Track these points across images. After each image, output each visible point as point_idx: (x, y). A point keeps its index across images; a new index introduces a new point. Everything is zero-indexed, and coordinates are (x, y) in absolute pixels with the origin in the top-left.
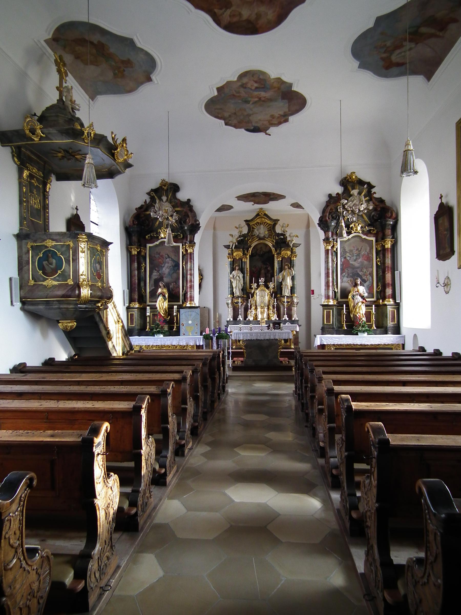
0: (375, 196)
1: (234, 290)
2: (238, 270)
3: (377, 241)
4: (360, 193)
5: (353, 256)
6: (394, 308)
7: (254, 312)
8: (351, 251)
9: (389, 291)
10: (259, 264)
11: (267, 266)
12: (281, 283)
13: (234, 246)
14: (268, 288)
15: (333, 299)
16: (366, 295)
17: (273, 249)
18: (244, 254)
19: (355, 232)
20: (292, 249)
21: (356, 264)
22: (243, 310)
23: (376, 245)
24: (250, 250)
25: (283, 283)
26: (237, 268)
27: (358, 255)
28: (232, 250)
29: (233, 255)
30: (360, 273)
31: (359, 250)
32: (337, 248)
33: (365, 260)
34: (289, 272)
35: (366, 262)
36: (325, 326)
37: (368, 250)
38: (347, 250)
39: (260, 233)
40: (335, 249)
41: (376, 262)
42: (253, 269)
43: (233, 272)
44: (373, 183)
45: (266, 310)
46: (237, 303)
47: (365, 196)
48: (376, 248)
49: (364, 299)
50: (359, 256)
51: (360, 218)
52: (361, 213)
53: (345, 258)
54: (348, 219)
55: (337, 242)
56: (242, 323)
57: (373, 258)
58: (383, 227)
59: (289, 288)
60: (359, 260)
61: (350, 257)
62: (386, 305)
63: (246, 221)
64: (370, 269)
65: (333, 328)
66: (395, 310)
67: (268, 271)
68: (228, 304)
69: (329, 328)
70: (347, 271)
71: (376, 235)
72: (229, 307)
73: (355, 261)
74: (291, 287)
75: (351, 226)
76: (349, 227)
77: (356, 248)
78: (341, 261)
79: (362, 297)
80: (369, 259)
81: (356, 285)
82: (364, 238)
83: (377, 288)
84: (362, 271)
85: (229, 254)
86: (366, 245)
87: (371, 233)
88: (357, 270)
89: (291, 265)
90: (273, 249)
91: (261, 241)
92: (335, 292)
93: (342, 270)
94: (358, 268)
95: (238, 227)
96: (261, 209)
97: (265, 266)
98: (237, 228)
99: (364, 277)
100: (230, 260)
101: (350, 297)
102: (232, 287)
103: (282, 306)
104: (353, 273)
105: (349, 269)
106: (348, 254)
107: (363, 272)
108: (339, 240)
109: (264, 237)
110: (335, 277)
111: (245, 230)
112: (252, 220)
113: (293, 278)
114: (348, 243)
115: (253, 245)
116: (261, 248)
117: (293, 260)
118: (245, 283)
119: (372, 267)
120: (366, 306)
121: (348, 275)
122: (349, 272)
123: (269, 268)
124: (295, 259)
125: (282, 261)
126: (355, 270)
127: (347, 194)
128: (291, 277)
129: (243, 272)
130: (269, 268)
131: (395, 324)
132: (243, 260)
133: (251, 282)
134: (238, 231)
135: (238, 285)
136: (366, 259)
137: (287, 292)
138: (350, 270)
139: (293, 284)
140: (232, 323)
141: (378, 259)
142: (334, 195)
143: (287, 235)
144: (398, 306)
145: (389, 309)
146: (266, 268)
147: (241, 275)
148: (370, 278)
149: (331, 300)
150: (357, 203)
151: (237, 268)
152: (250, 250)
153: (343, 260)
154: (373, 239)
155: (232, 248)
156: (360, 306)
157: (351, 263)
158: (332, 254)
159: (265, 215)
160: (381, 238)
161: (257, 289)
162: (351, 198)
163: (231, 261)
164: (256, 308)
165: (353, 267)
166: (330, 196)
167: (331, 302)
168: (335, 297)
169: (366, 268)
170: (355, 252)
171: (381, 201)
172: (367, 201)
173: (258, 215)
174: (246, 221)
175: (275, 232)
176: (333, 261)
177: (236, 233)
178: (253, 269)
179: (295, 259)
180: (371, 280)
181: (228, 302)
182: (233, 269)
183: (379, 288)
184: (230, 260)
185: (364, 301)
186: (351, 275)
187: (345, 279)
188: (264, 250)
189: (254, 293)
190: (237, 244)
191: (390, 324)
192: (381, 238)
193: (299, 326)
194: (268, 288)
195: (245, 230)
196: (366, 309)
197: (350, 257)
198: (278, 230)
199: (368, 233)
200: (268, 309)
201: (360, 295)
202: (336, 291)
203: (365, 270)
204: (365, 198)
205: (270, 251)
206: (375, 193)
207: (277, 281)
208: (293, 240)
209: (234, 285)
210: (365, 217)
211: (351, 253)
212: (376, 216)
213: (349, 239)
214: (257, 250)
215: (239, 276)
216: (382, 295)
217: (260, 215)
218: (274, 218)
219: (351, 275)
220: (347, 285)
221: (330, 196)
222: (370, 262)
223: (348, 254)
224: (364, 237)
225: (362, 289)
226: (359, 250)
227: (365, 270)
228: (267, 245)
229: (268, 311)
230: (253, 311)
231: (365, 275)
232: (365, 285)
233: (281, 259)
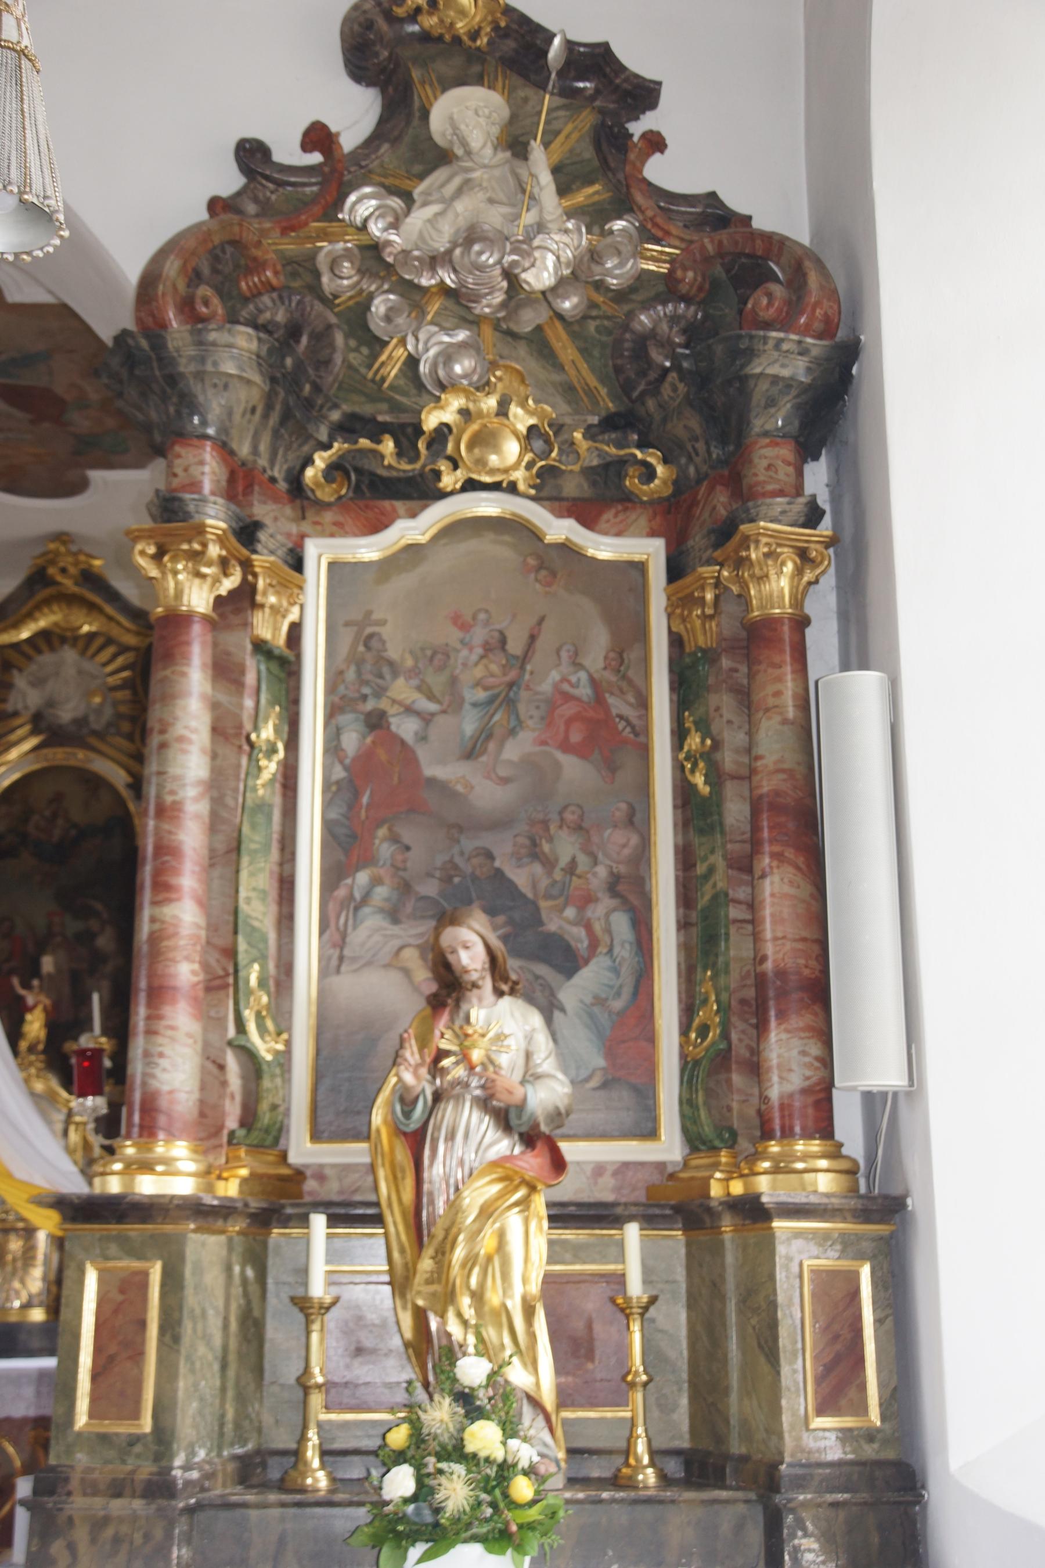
0: (657, 170)
3: (675, 571)
4: (515, 144)
5: (455, 705)
6: (848, 1246)
8: (438, 656)
9: (785, 1053)
11: (94, 924)
15: (206, 1131)
16: (548, 1094)
19: (471, 485)
21: (485, 790)
23: (680, 604)
27: (505, 698)
30: (521, 877)
31: (515, 646)
32: (295, 632)
33: (566, 747)
35: (575, 772)
36: (81, 1458)
37: (595, 659)
38: (393, 653)
40: (267, 628)
41: (679, 768)
44: (636, 58)
47: (566, 179)
48: (676, 641)
49: (530, 1139)
50: (510, 704)
51: (523, 359)
52: (528, 320)
53: (376, 722)
54: (412, 362)
55: (297, 564)
57: (642, 733)
58: (722, 407)
60: (514, 750)
61: (427, 719)
62: (753, 1211)
64: (618, 841)
65: (161, 1488)
66: (865, 1272)
69: (117, 1489)
70: (385, 850)
71: (673, 518)
73: (470, 753)
75: (431, 421)
76: (418, 431)
77: (479, 635)
78: (333, 748)
79: (505, 1117)
80: (608, 736)
81: (449, 988)
82: (566, 549)
83: (684, 1031)
84: (534, 853)
86: (588, 607)
87: (627, 500)
88: (486, 840)
91: (58, 755)
92: (248, 1055)
93: (345, 849)
94: (498, 824)
96: (62, 537)
97: (74, 926)
99: (562, 920)
101: (377, 1118)
104: (448, 873)
105: (407, 835)
106: (402, 689)
107: (549, 864)
108: (318, 554)
109: (81, 722)
110: (258, 911)
114: (403, 582)
116: (58, 798)
119: (638, 819)
120: (561, 1216)
121: (405, 888)
122: (416, 859)
126: (469, 844)
127: (405, 150)
131: (870, 1435)
136: (576, 737)
138: (422, 845)
141: (694, 741)
142: (288, 152)
144: (883, 1213)
145: (800, 1254)
146: (87, 937)
148: (621, 924)
149: (180, 1151)
150: (494, 218)
153: (351, 741)
154: (651, 551)
156: (487, 1212)
157: (431, 770)
158: (225, 671)
159: (91, 579)
160: (703, 528)
162: (440, 175)
165: (458, 822)
166: (251, 155)
167: (175, 1171)
168: (249, 1118)
169: (578, 828)
170: (476, 674)
171: (713, 214)
172: (595, 217)
176: (228, 732)
180: (625, 952)
183: (704, 1031)
185: (533, 1163)
186: (430, 889)
187: (370, 930)
191: (817, 1436)
192: (703, 528)
196: (556, 1251)
197: (427, 719)
199: (599, 499)
201: (485, 1103)
202: (265, 1048)
203: (565, 847)
204: (563, 191)
206: (656, 143)
210: (567, 351)
211: (437, 681)
212: (666, 345)
213: (412, 551)
216: (729, 1111)
219: (430, 889)
220: (391, 991)
221: (251, 155)
222: (611, 767)
223: (402, 689)
224: (559, 529)
225: (506, 1030)
226: (515, 646)
227: (565, 847)
231: (561, 894)
232: (573, 993)
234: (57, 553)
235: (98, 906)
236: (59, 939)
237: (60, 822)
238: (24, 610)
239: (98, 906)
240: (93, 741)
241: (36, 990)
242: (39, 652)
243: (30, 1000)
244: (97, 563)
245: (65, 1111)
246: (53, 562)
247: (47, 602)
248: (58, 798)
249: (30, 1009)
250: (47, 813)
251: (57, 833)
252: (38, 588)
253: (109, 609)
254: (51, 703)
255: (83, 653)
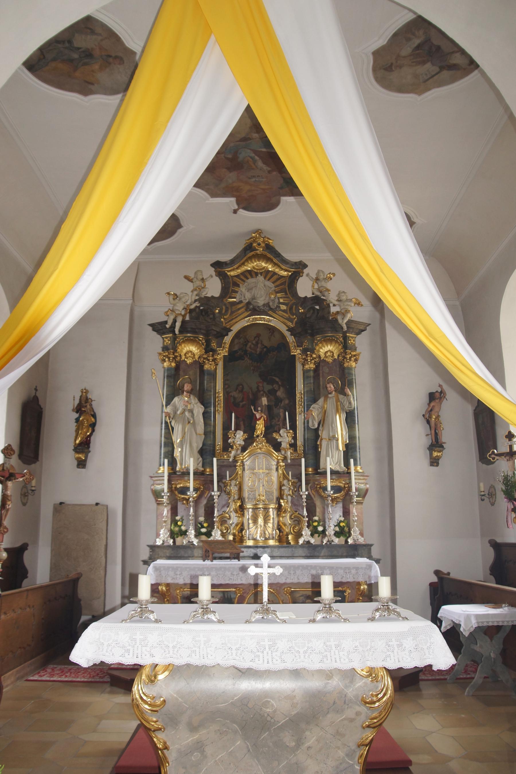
1: (177, 453)
2: (191, 392)
7: (234, 519)
10: (252, 381)
11: (276, 386)
12: (316, 433)
13: (178, 325)
14: (277, 446)
17: (291, 339)
18: (208, 349)
20: (345, 338)
22: (202, 511)
24: (228, 339)
25: (324, 434)
26: (187, 387)
28: (175, 337)
29: (175, 351)
34: (338, 400)
39: (254, 298)
42: (235, 394)
43: (176, 400)
45: (272, 513)
46: (184, 490)
56: (198, 552)
59: (341, 448)
63: (217, 265)
67: (278, 401)
68: (157, 494)
72: (159, 504)
74: (347, 446)
85: (165, 348)
89: (345, 380)
90: (291, 339)
95: (192, 276)
96: (259, 231)
97: (268, 387)
98: (191, 281)
100: (166, 364)
102: (169, 444)
103: (318, 503)
109: (268, 305)
111: (214, 288)
112: (233, 262)
113: (350, 419)
115: (236, 328)
116: (258, 336)
117: (350, 368)
118: (209, 432)
123: (279, 394)
124: (353, 364)
125: (316, 370)
128: (344, 416)
129: (203, 401)
130: (279, 394)
132: (206, 367)
133: (226, 427)
134: (190, 286)
135: (187, 437)
137: (331, 461)
139: (352, 438)
140: (168, 552)
143: (332, 297)
147: (199, 409)
151: (187, 387)
152: (228, 339)
155: (173, 332)
159: (269, 248)
161: (244, 449)
163: (169, 369)
164: (242, 509)
173: (249, 248)
174: (217, 265)
175: (294, 293)
177: (188, 295)
178: (235, 394)
179: (353, 364)
181: (159, 487)
182: (173, 392)
184: (166, 364)
188: (266, 343)
189: (235, 461)
190: (187, 318)
193: (378, 561)
194: (277, 446)
195: (214, 288)
198: (305, 288)
200: (279, 509)
205: (284, 345)
207: (307, 428)
208: (347, 311)
209: (177, 439)
214: (247, 342)
215: (191, 411)
217: (257, 247)
218: (292, 257)
228: (272, 330)
229: (278, 515)
230: (233, 515)
233: (312, 366)
234: (256, 237)
235: (277, 379)
236: (262, 392)
237: (259, 345)
238: (242, 262)
239: (277, 379)
240: (270, 312)
241: (260, 412)
242: (248, 279)
243: (258, 416)
244: (271, 241)
245: (276, 460)
246: (254, 241)
247: (250, 258)
248: (258, 336)
249: (260, 419)
250: (254, 342)
251: (258, 350)
252: (249, 251)
253: (275, 260)
254: (254, 298)
255: (265, 278)
